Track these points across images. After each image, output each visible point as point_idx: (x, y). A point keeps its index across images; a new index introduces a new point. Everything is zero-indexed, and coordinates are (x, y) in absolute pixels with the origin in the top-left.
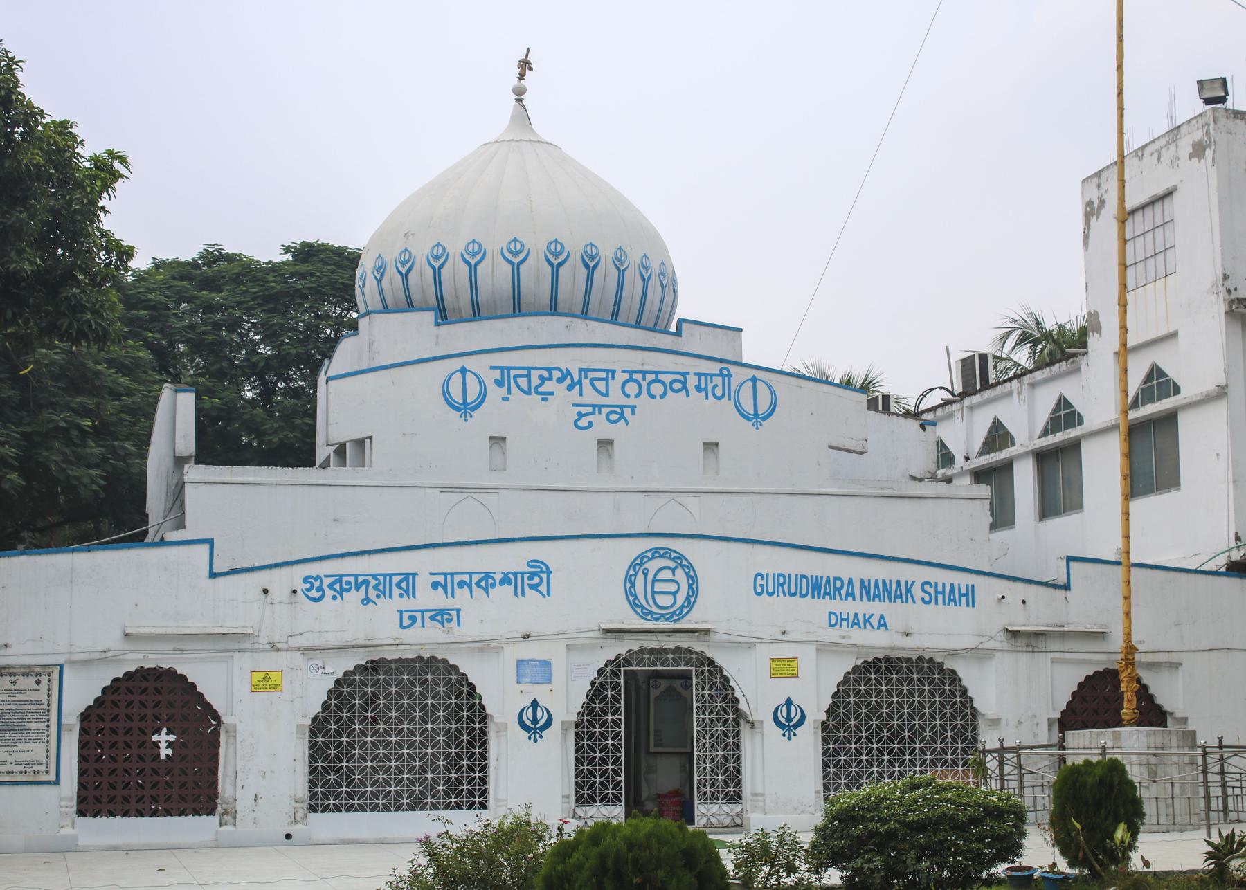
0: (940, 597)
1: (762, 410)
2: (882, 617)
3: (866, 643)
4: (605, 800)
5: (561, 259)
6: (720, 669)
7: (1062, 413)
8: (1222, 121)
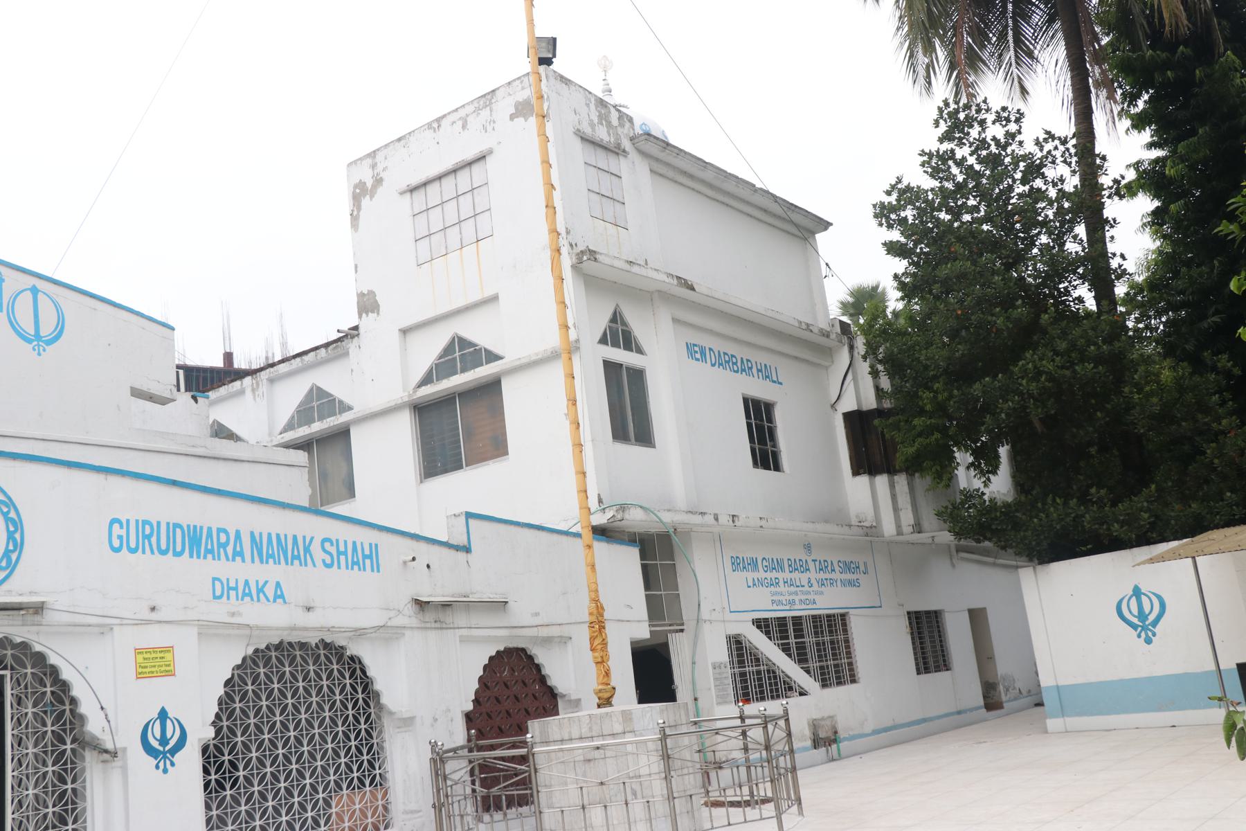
0: (342, 558)
1: (47, 329)
2: (278, 584)
3: (260, 623)
7: (315, 404)
8: (552, 80)
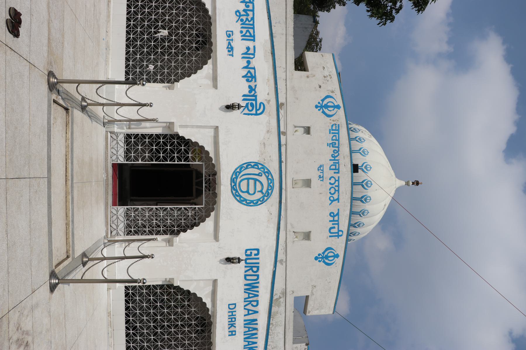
4: (127, 152)
5: (365, 186)
6: (203, 221)
